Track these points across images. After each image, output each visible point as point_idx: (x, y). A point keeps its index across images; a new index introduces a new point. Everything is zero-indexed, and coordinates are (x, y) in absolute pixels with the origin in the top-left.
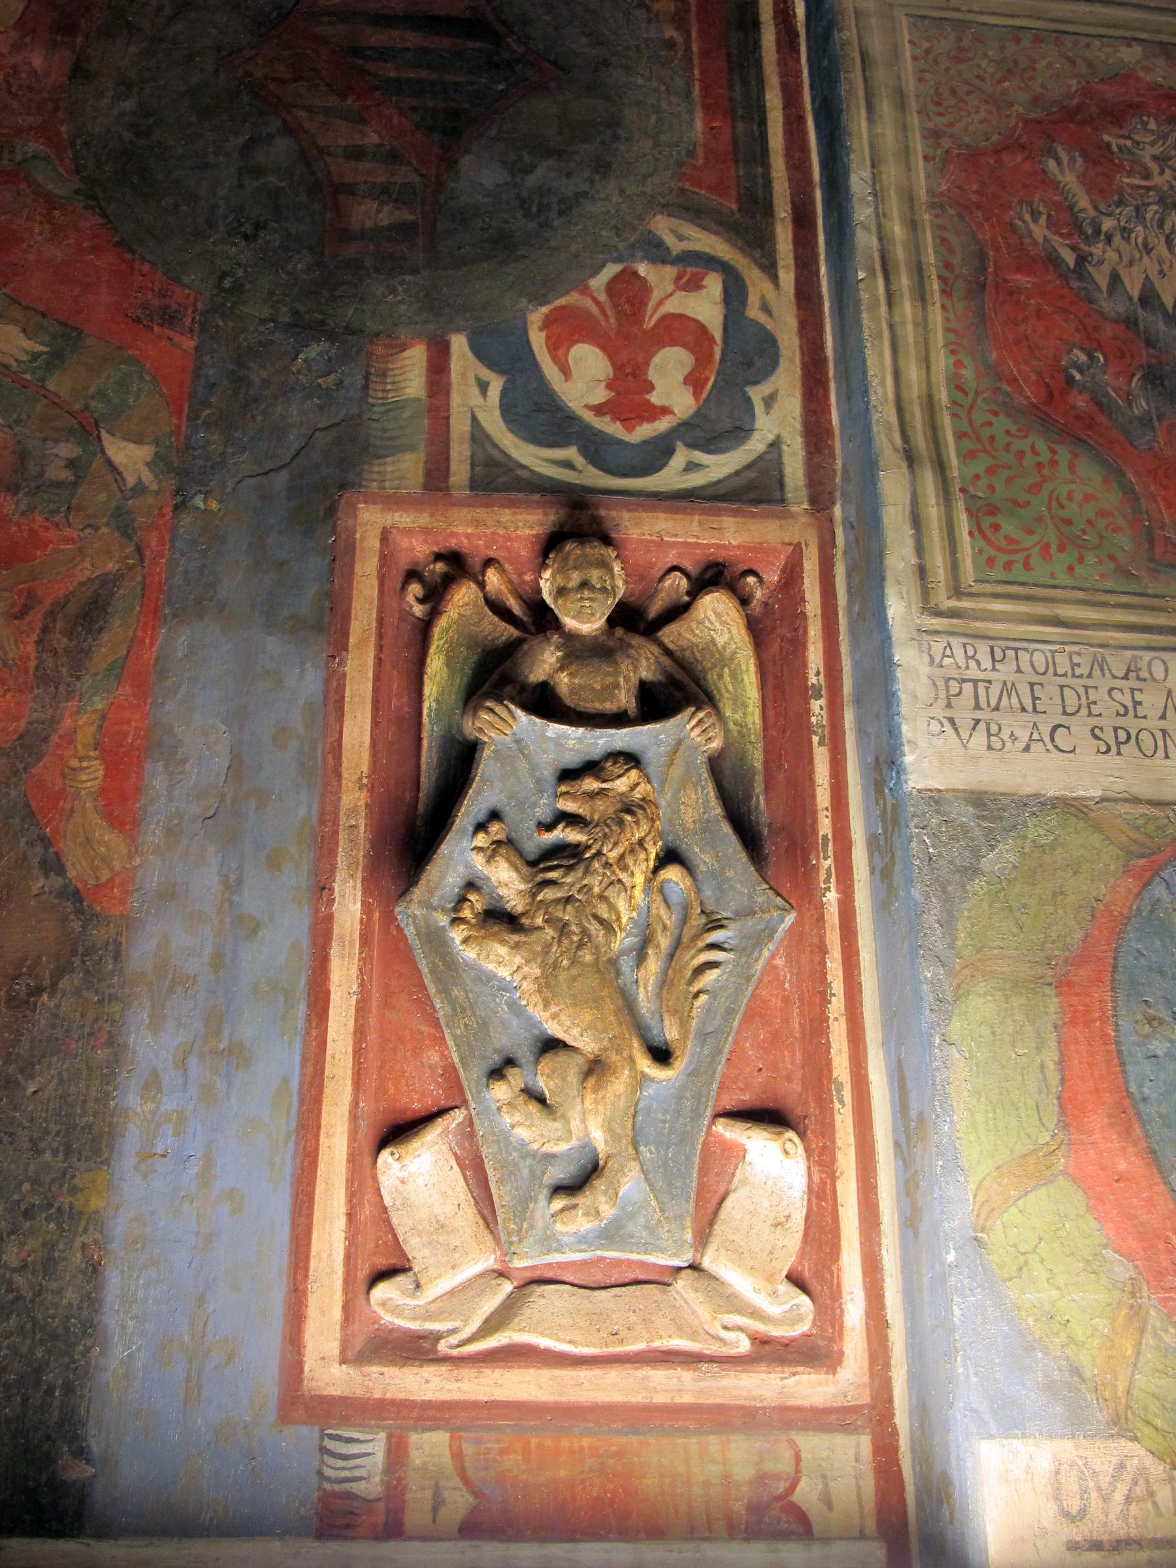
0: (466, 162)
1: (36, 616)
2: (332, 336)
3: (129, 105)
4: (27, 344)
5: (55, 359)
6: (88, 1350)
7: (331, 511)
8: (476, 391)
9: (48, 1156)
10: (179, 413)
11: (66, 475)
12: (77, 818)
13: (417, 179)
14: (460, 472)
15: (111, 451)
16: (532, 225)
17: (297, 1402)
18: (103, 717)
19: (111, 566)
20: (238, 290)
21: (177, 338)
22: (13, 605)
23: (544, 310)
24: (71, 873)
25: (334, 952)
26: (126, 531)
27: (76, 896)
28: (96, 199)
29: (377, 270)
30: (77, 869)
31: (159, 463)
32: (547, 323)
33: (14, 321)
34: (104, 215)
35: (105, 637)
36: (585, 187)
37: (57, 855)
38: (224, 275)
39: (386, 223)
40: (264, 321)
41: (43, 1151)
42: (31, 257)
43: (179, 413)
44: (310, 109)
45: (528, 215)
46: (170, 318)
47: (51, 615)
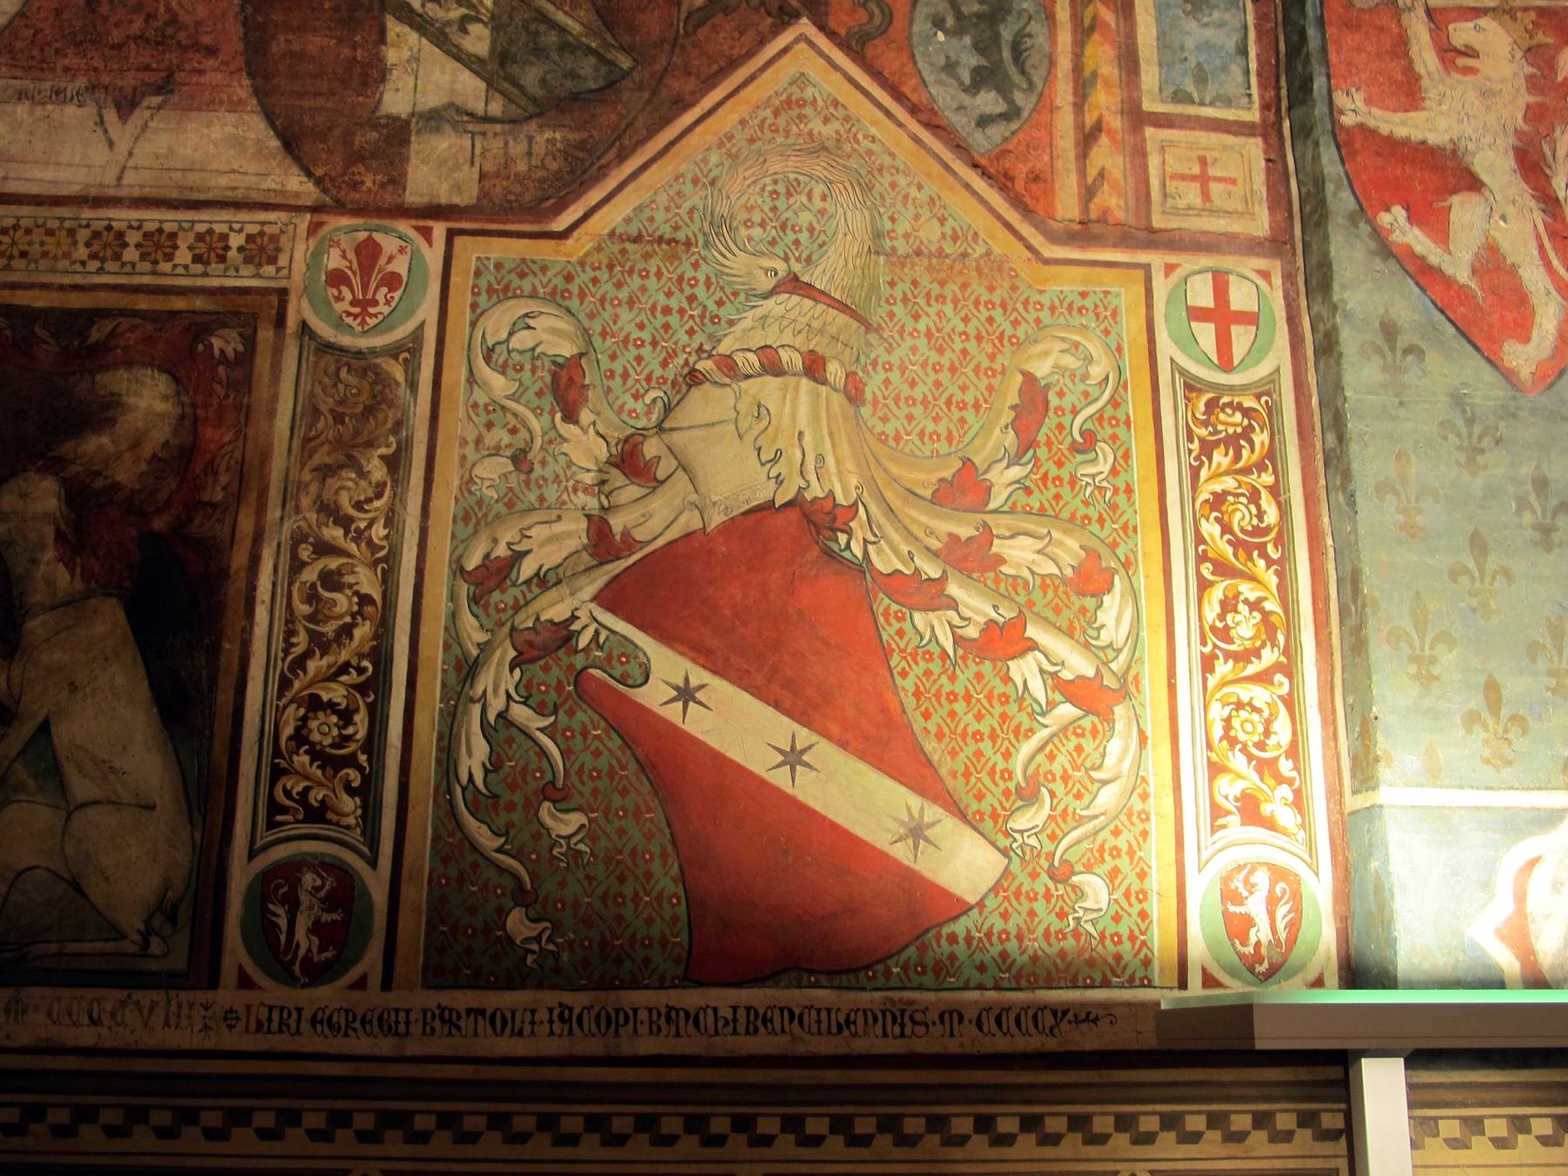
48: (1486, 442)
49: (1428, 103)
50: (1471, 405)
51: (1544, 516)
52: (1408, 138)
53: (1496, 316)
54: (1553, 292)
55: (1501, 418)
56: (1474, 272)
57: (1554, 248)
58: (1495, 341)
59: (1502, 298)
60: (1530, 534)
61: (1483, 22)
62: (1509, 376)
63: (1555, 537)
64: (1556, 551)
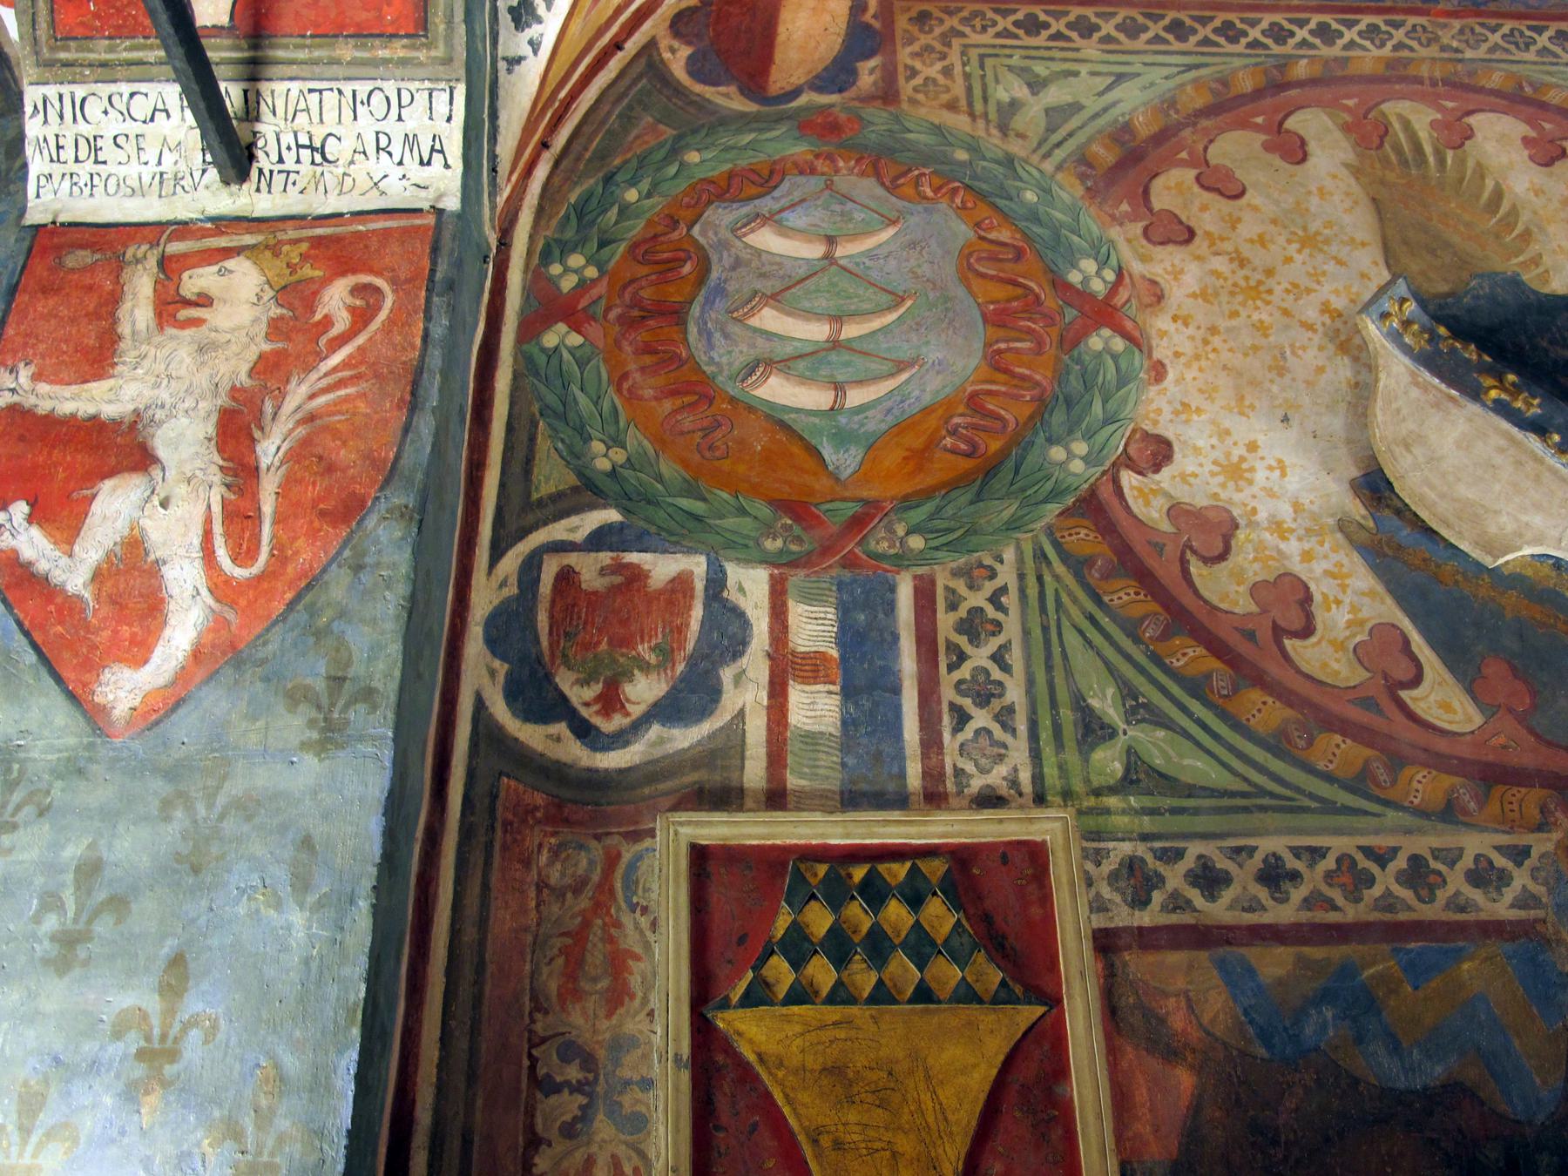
48: (29, 811)
49: (119, 368)
50: (22, 762)
51: (75, 921)
52: (73, 416)
53: (106, 634)
54: (204, 592)
55: (60, 777)
56: (98, 576)
57: (227, 535)
58: (92, 666)
59: (122, 607)
60: (45, 947)
61: (230, 264)
62: (94, 716)
63: (81, 952)
64: (77, 972)
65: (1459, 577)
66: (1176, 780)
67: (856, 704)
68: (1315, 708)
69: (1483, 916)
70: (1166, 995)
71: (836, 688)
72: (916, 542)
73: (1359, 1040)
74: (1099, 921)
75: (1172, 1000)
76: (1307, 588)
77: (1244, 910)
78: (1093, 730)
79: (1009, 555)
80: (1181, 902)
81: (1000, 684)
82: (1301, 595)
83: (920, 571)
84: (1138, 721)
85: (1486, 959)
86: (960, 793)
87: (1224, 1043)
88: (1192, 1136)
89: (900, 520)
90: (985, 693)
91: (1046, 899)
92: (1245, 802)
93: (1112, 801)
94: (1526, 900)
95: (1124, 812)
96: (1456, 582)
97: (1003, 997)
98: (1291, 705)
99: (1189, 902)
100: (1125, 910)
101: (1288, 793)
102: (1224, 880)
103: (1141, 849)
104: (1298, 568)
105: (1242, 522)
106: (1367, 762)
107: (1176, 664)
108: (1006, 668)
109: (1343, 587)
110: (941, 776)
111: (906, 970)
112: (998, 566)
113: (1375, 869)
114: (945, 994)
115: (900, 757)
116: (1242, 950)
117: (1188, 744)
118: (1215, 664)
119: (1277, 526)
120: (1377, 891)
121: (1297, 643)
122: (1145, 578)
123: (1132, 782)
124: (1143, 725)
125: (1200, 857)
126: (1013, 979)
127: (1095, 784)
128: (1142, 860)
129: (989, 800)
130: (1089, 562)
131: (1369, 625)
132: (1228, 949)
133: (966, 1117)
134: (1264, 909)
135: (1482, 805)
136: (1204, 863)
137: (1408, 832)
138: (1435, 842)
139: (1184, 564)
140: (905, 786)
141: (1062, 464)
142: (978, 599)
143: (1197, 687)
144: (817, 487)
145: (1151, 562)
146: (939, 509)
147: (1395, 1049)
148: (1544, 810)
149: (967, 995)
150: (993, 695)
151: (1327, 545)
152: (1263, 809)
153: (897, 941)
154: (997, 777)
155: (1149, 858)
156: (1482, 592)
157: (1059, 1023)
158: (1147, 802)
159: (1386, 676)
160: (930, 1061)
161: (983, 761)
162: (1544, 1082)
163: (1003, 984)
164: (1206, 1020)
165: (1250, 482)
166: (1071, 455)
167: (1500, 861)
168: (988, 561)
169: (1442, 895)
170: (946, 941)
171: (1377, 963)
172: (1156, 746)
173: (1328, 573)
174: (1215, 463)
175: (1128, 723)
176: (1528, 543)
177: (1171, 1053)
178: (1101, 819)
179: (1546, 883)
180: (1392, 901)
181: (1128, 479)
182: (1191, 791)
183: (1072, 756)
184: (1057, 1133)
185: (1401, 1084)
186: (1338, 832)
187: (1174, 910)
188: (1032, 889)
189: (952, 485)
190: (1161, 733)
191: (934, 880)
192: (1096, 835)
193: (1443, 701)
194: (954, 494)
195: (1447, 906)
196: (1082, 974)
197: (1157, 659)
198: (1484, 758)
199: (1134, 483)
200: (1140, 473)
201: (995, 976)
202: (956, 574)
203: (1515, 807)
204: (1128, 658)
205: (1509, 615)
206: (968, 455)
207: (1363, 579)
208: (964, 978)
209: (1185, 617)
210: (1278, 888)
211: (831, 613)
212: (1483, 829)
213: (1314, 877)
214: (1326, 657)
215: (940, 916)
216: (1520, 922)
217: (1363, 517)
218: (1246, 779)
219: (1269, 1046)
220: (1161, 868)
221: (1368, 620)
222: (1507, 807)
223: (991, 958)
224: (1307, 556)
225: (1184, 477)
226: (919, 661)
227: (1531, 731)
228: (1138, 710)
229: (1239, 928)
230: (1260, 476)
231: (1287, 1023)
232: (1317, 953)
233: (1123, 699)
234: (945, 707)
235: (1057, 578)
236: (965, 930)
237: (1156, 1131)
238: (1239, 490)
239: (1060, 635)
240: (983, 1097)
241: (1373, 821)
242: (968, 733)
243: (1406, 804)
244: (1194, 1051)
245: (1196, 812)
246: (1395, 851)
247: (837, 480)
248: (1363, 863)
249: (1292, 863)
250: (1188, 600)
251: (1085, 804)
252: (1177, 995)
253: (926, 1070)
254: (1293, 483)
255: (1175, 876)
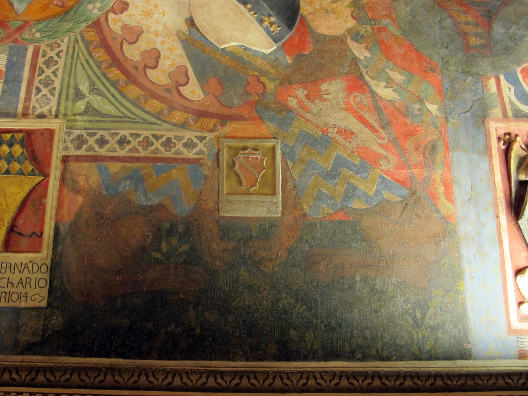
0: (494, 26)
1: (421, 149)
2: (472, 76)
3: (408, 9)
4: (401, 77)
5: (409, 81)
6: (466, 320)
7: (483, 123)
8: (508, 90)
9: (449, 278)
10: (441, 96)
11: (419, 113)
12: (440, 200)
13: (484, 31)
14: (510, 114)
15: (428, 107)
16: (513, 44)
17: (511, 331)
18: (442, 175)
19: (435, 137)
20: (447, 62)
21: (436, 76)
22: (415, 147)
23: (520, 68)
24: (442, 213)
25: (502, 231)
26: (436, 128)
27: (444, 218)
28: (406, 36)
29: (479, 57)
30: (443, 212)
31: (439, 109)
32: (522, 71)
33: (396, 71)
34: (410, 41)
35: (438, 155)
36: (524, 33)
37: (438, 209)
38: (443, 58)
39: (478, 44)
40: (456, 71)
41: (448, 277)
42: (395, 53)
43: (441, 96)
44: (453, 10)
45: (512, 42)
46: (433, 71)
47: (424, 149)
65: (211, 51)
66: (100, 112)
67: (7, 86)
68: (151, 91)
69: (184, 157)
70: (80, 175)
71: (2, 81)
72: (38, 35)
73: (135, 191)
74: (64, 153)
75: (82, 177)
76: (160, 53)
77: (110, 151)
78: (79, 95)
79: (66, 40)
80: (91, 148)
81: (53, 81)
82: (157, 55)
83: (36, 44)
84: (93, 94)
85: (181, 169)
86: (33, 114)
87: (95, 190)
88: (78, 215)
89: (35, 28)
90: (47, 83)
91: (51, 146)
92: (122, 119)
93: (78, 118)
94: (201, 152)
95: (81, 121)
96: (210, 53)
97: (33, 174)
98: (143, 90)
99: (94, 149)
100: (74, 150)
101: (134, 117)
102: (107, 142)
103: (83, 133)
104: (158, 46)
105: (145, 31)
106: (162, 108)
107: (110, 76)
108: (56, 76)
109: (172, 53)
110: (28, 109)
111: (4, 165)
112: (61, 43)
113: (154, 141)
114: (13, 173)
115: (17, 102)
116: (106, 163)
117: (107, 101)
118: (123, 76)
119: (156, 34)
120: (153, 147)
121: (151, 70)
122: (108, 49)
123: (87, 112)
124: (95, 95)
125: (102, 135)
126: (37, 169)
127: (75, 112)
128: (83, 136)
129: (42, 116)
130: (91, 43)
131: (176, 66)
132: (102, 162)
133: (14, 206)
134: (116, 151)
135: (195, 123)
136: (102, 137)
137: (169, 130)
138: (176, 134)
139: (122, 44)
140: (17, 111)
141: (91, 10)
142: (53, 54)
143: (114, 84)
144: (10, 16)
145: (111, 43)
146: (47, 24)
147: (145, 194)
148: (215, 126)
149: (21, 173)
150: (50, 84)
151: (171, 40)
152: (125, 122)
153: (3, 157)
154: (45, 110)
155: (85, 135)
156: (217, 56)
157: (48, 182)
158: (90, 118)
159: (176, 82)
160: (7, 191)
161: (42, 104)
162: (188, 205)
163: (33, 170)
164: (90, 183)
165: (152, 18)
166: (95, 7)
167: (195, 140)
168: (59, 42)
169: (173, 150)
170: (18, 157)
171: (147, 168)
172: (97, 102)
173: (169, 49)
174: (142, 11)
175: (90, 94)
176: (232, 41)
177: (77, 192)
178: (73, 123)
179: (208, 148)
180: (157, 151)
181: (111, 16)
182: (104, 115)
183: (70, 104)
184: (40, 213)
185: (145, 203)
186: (146, 129)
187: (88, 151)
188: (48, 143)
189: (54, 16)
190: (99, 97)
191: (19, 139)
192: (71, 128)
193: (193, 91)
194: (53, 20)
195: (174, 153)
196: (56, 168)
197: (104, 75)
198: (201, 109)
199: (113, 17)
200: (116, 14)
201: (31, 167)
202: (47, 45)
203: (206, 124)
204: (95, 74)
205: (223, 64)
206: (61, 7)
207: (179, 50)
208: (21, 168)
209: (116, 61)
210: (122, 146)
211: (5, 57)
212: (192, 130)
213: (134, 143)
214: (158, 77)
215: (18, 149)
216: (195, 159)
217: (186, 31)
218: (122, 113)
219: (107, 191)
220: (88, 138)
221: (176, 64)
222: (203, 124)
223: (31, 163)
224: (163, 43)
225: (130, 16)
226: (30, 73)
227: (219, 101)
228: (94, 90)
229: (107, 157)
230: (155, 16)
231: (115, 185)
232: (128, 165)
233: (90, 86)
234: (34, 87)
235: (80, 48)
236: (24, 154)
237: (68, 213)
238: (147, 20)
239: (76, 66)
240: (20, 202)
241: (159, 127)
242: (40, 96)
243: (171, 122)
244: (85, 191)
245: (104, 122)
246: (163, 136)
247: (17, 14)
248: (152, 139)
249: (129, 138)
250: (119, 56)
251: (70, 118)
252: (83, 175)
253: (5, 194)
254: (166, 19)
255: (92, 141)
